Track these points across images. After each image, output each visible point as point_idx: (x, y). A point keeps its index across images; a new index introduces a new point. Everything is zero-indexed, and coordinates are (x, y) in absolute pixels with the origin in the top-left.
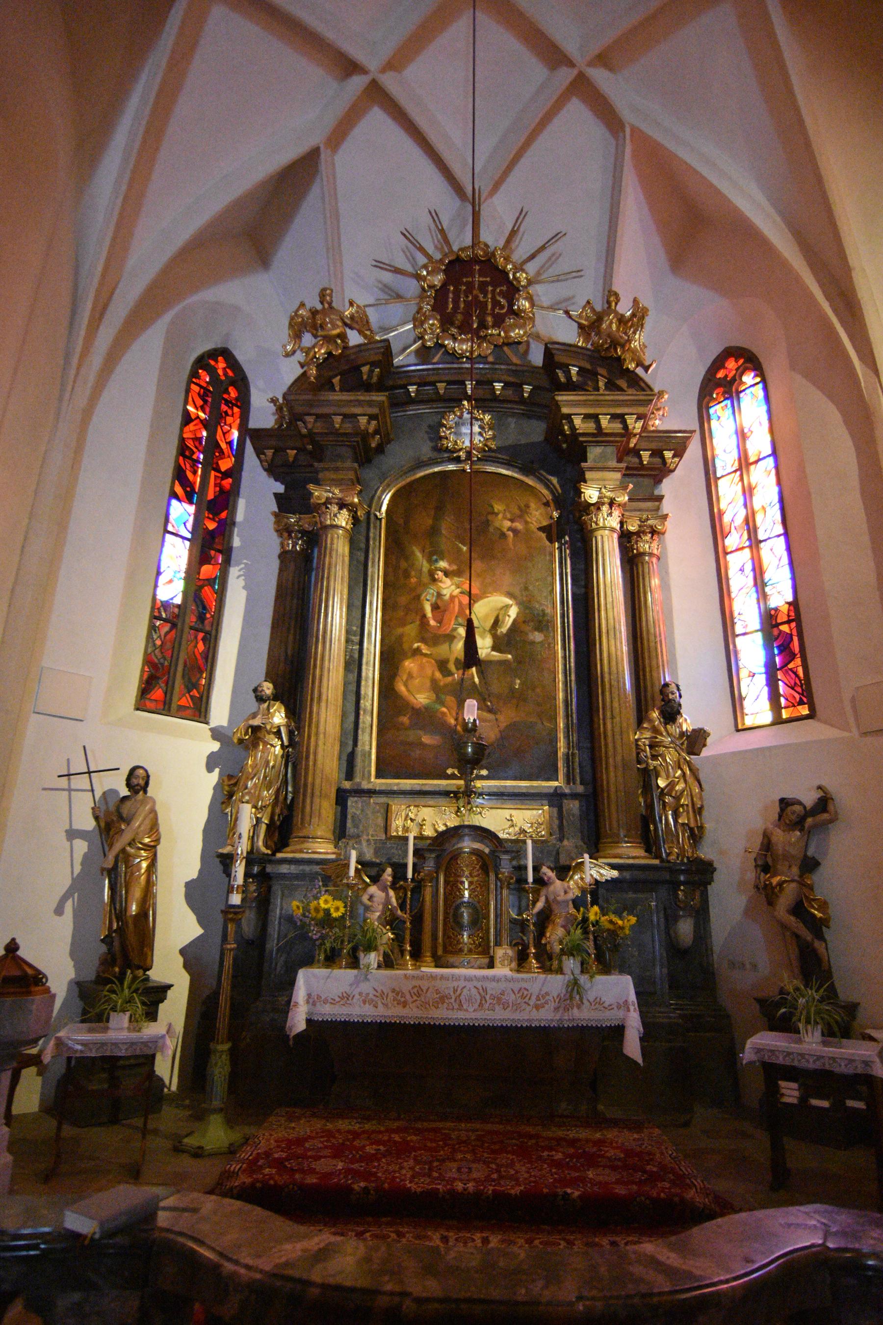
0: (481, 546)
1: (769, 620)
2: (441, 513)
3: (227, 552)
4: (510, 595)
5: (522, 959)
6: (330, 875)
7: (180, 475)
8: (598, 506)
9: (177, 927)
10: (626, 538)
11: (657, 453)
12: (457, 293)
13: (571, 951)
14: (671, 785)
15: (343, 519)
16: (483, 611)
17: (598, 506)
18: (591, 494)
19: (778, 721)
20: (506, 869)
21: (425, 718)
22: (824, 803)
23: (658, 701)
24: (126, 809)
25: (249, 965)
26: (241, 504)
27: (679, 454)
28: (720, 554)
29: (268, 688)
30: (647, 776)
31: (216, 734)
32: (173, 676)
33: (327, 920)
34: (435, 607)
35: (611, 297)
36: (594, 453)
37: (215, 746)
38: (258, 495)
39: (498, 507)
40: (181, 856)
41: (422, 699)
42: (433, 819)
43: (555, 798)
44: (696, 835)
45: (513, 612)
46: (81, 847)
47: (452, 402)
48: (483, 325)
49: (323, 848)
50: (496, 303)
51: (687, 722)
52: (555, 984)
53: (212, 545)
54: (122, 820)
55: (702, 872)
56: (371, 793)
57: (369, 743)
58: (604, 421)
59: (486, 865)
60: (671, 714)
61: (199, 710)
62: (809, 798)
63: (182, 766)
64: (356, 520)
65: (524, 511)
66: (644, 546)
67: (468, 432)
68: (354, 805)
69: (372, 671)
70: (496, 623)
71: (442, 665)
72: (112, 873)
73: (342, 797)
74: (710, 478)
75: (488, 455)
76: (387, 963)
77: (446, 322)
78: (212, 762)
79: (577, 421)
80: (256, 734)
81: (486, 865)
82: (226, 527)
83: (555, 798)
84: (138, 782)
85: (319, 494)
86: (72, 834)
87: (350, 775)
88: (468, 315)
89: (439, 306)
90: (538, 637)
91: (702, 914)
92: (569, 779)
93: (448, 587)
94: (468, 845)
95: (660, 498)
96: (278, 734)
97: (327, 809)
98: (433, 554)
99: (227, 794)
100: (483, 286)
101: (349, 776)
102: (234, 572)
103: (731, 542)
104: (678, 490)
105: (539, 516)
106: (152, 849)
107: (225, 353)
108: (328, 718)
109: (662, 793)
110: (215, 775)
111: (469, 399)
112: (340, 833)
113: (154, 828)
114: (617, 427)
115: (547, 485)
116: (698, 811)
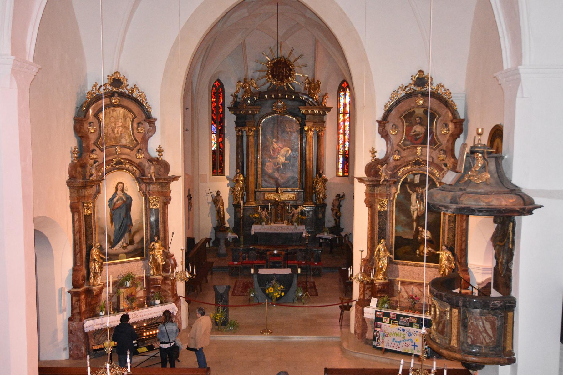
1: (345, 152)
3: (224, 134)
4: (289, 147)
5: (288, 224)
6: (255, 209)
7: (213, 119)
8: (308, 130)
9: (227, 217)
12: (276, 69)
13: (296, 222)
15: (251, 134)
18: (306, 128)
19: (343, 176)
22: (344, 196)
24: (217, 198)
25: (242, 224)
26: (226, 121)
28: (338, 134)
29: (238, 170)
31: (228, 178)
32: (218, 167)
33: (256, 218)
34: (273, 151)
36: (307, 117)
38: (230, 119)
40: (226, 205)
41: (270, 171)
46: (210, 205)
48: (283, 79)
49: (253, 204)
50: (286, 72)
52: (293, 227)
53: (221, 133)
54: (217, 200)
55: (324, 206)
58: (310, 112)
60: (320, 175)
61: (222, 173)
62: (342, 195)
63: (222, 186)
68: (258, 194)
71: (274, 164)
73: (255, 192)
74: (338, 114)
76: (266, 224)
77: (274, 77)
78: (228, 185)
82: (223, 127)
84: (218, 193)
86: (209, 203)
87: (256, 188)
88: (279, 76)
89: (272, 73)
91: (324, 213)
93: (275, 146)
96: (242, 181)
99: (232, 191)
100: (283, 68)
102: (226, 139)
103: (341, 131)
104: (329, 118)
106: (223, 205)
107: (218, 80)
108: (252, 179)
110: (229, 188)
112: (255, 199)
113: (223, 202)
116: (324, 195)
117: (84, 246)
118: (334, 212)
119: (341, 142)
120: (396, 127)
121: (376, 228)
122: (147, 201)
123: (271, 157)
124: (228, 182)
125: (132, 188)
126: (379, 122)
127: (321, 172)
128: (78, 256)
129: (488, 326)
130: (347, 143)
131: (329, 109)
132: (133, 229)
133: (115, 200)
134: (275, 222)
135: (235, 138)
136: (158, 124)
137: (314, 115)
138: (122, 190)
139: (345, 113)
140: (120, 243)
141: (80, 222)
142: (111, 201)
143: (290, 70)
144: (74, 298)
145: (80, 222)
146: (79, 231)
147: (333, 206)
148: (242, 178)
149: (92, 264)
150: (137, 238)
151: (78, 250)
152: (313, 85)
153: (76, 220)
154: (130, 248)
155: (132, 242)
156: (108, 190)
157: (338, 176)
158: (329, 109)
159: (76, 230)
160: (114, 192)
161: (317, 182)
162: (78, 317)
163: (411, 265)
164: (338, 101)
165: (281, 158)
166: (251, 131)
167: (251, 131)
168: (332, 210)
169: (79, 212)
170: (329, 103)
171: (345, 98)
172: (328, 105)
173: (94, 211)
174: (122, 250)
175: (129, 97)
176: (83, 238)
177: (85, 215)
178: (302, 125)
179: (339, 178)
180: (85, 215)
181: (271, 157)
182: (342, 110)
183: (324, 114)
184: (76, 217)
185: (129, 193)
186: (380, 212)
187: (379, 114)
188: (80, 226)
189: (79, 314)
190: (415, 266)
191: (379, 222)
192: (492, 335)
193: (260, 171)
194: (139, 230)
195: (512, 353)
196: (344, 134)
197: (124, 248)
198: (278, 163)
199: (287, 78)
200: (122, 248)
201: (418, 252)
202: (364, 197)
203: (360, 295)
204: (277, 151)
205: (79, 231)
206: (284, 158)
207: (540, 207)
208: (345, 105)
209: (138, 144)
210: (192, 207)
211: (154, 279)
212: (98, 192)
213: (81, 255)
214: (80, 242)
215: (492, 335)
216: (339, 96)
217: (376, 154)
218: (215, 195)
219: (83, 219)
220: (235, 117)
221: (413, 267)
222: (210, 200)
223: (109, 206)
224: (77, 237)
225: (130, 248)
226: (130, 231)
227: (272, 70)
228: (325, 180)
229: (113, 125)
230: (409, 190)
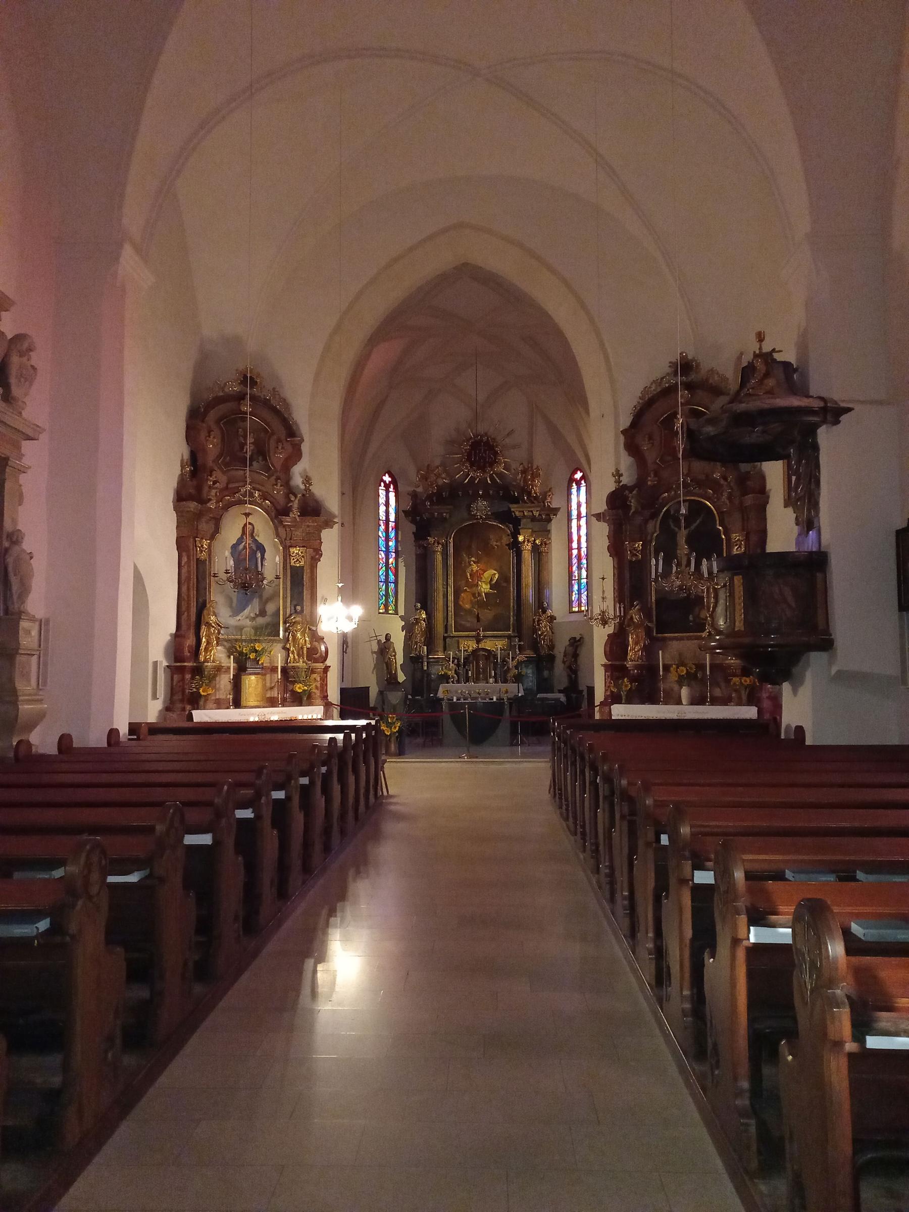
0: (487, 552)
2: (471, 539)
5: (496, 682)
8: (524, 542)
9: (401, 677)
10: (536, 549)
11: (548, 515)
14: (542, 633)
15: (440, 548)
16: (487, 575)
17: (524, 542)
18: (521, 538)
20: (492, 659)
21: (469, 612)
23: (541, 605)
27: (556, 515)
30: (535, 631)
35: (531, 462)
36: (523, 521)
37: (403, 623)
39: (491, 537)
40: (400, 659)
41: (467, 606)
42: (472, 645)
43: (509, 637)
44: (552, 647)
45: (497, 576)
47: (475, 497)
50: (490, 457)
51: (549, 612)
55: (552, 658)
56: (453, 637)
57: (452, 622)
59: (487, 658)
60: (544, 612)
64: (443, 545)
65: (501, 538)
66: (542, 549)
67: (481, 507)
69: (451, 598)
70: (491, 580)
71: (474, 595)
72: (387, 664)
73: (445, 638)
74: (569, 520)
75: (488, 517)
77: (472, 465)
79: (517, 513)
80: (417, 621)
81: (487, 658)
83: (509, 637)
84: (388, 637)
85: (431, 540)
86: (373, 652)
87: (446, 632)
89: (469, 459)
90: (505, 584)
91: (551, 669)
92: (513, 631)
93: (475, 567)
94: (482, 653)
95: (549, 531)
97: (441, 642)
98: (470, 555)
99: (408, 639)
101: (446, 632)
104: (556, 526)
105: (506, 540)
108: (439, 616)
109: (540, 635)
111: (481, 496)
112: (445, 649)
113: (394, 651)
114: (530, 514)
115: (509, 528)
116: (551, 641)
117: (193, 605)
118: (567, 664)
119: (575, 561)
120: (651, 438)
121: (627, 586)
122: (286, 556)
123: (467, 584)
124: (403, 623)
125: (265, 532)
126: (624, 432)
127: (546, 605)
128: (184, 617)
129: (787, 592)
130: (584, 561)
131: (555, 511)
132: (266, 595)
133: (241, 547)
134: (477, 680)
135: (414, 557)
136: (305, 448)
137: (533, 519)
138: (252, 535)
139: (579, 517)
140: (246, 612)
141: (189, 566)
142: (234, 547)
143: (496, 454)
144: (175, 676)
145: (189, 566)
146: (188, 579)
147: (565, 656)
148: (424, 616)
149: (204, 631)
150: (270, 608)
151: (184, 608)
152: (529, 471)
153: (183, 563)
154: (261, 621)
155: (262, 613)
156: (231, 532)
157: (572, 612)
158: (555, 511)
159: (183, 577)
160: (238, 534)
161: (539, 621)
162: (179, 705)
163: (681, 639)
164: (569, 500)
165: (484, 586)
166: (438, 543)
167: (438, 543)
168: (564, 662)
169: (188, 551)
170: (555, 502)
171: (578, 495)
172: (554, 506)
173: (210, 555)
174: (248, 622)
175: (266, 403)
176: (193, 593)
177: (197, 559)
178: (516, 533)
179: (574, 618)
180: (197, 559)
181: (467, 584)
182: (574, 513)
183: (550, 520)
184: (185, 559)
185: (260, 539)
186: (631, 561)
187: (625, 421)
188: (189, 572)
189: (182, 701)
190: (689, 638)
191: (631, 578)
192: (793, 605)
193: (451, 605)
194: (276, 595)
195: (827, 631)
196: (579, 548)
197: (253, 619)
198: (480, 594)
199: (491, 465)
200: (248, 620)
201: (691, 618)
202: (606, 543)
203: (606, 690)
204: (477, 576)
205: (188, 579)
206: (489, 586)
207: (849, 410)
208: (579, 505)
209: (276, 471)
210: (347, 646)
211: (294, 667)
212: (217, 530)
213: (189, 616)
214: (189, 596)
215: (793, 605)
216: (569, 494)
217: (621, 478)
218: (384, 640)
219: (193, 564)
220: (413, 528)
221: (686, 642)
222: (375, 647)
223: (232, 554)
224: (184, 589)
225: (261, 621)
226: (261, 597)
227: (469, 456)
228: (552, 618)
229: (242, 439)
230: (672, 526)
